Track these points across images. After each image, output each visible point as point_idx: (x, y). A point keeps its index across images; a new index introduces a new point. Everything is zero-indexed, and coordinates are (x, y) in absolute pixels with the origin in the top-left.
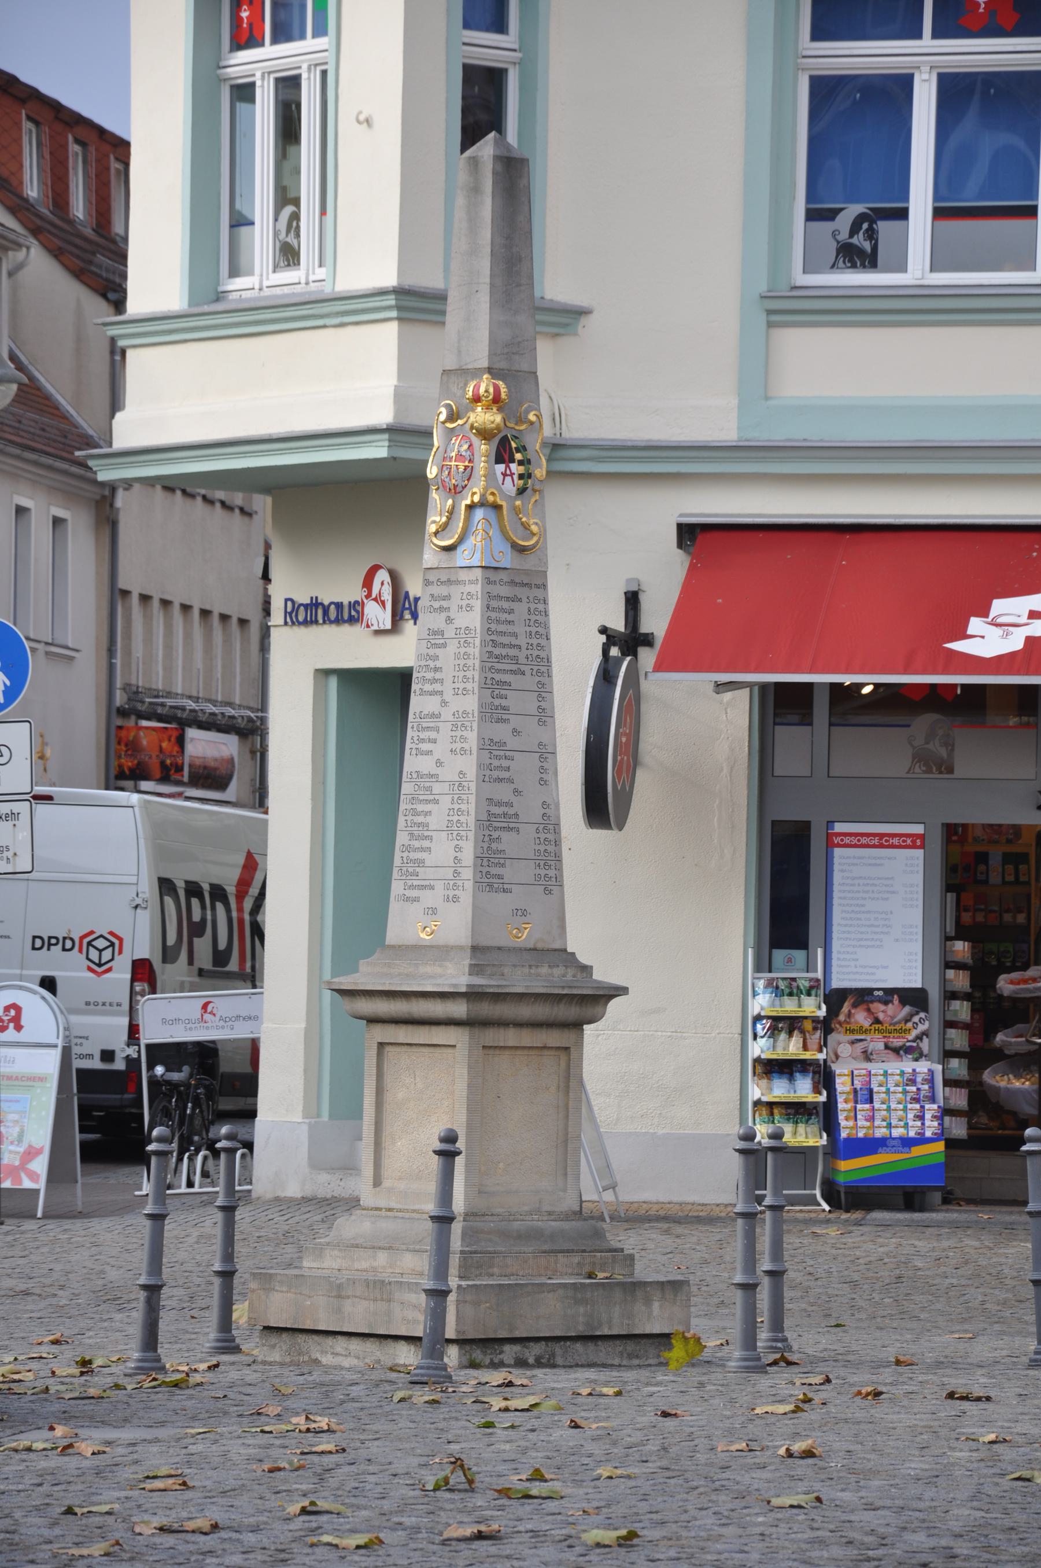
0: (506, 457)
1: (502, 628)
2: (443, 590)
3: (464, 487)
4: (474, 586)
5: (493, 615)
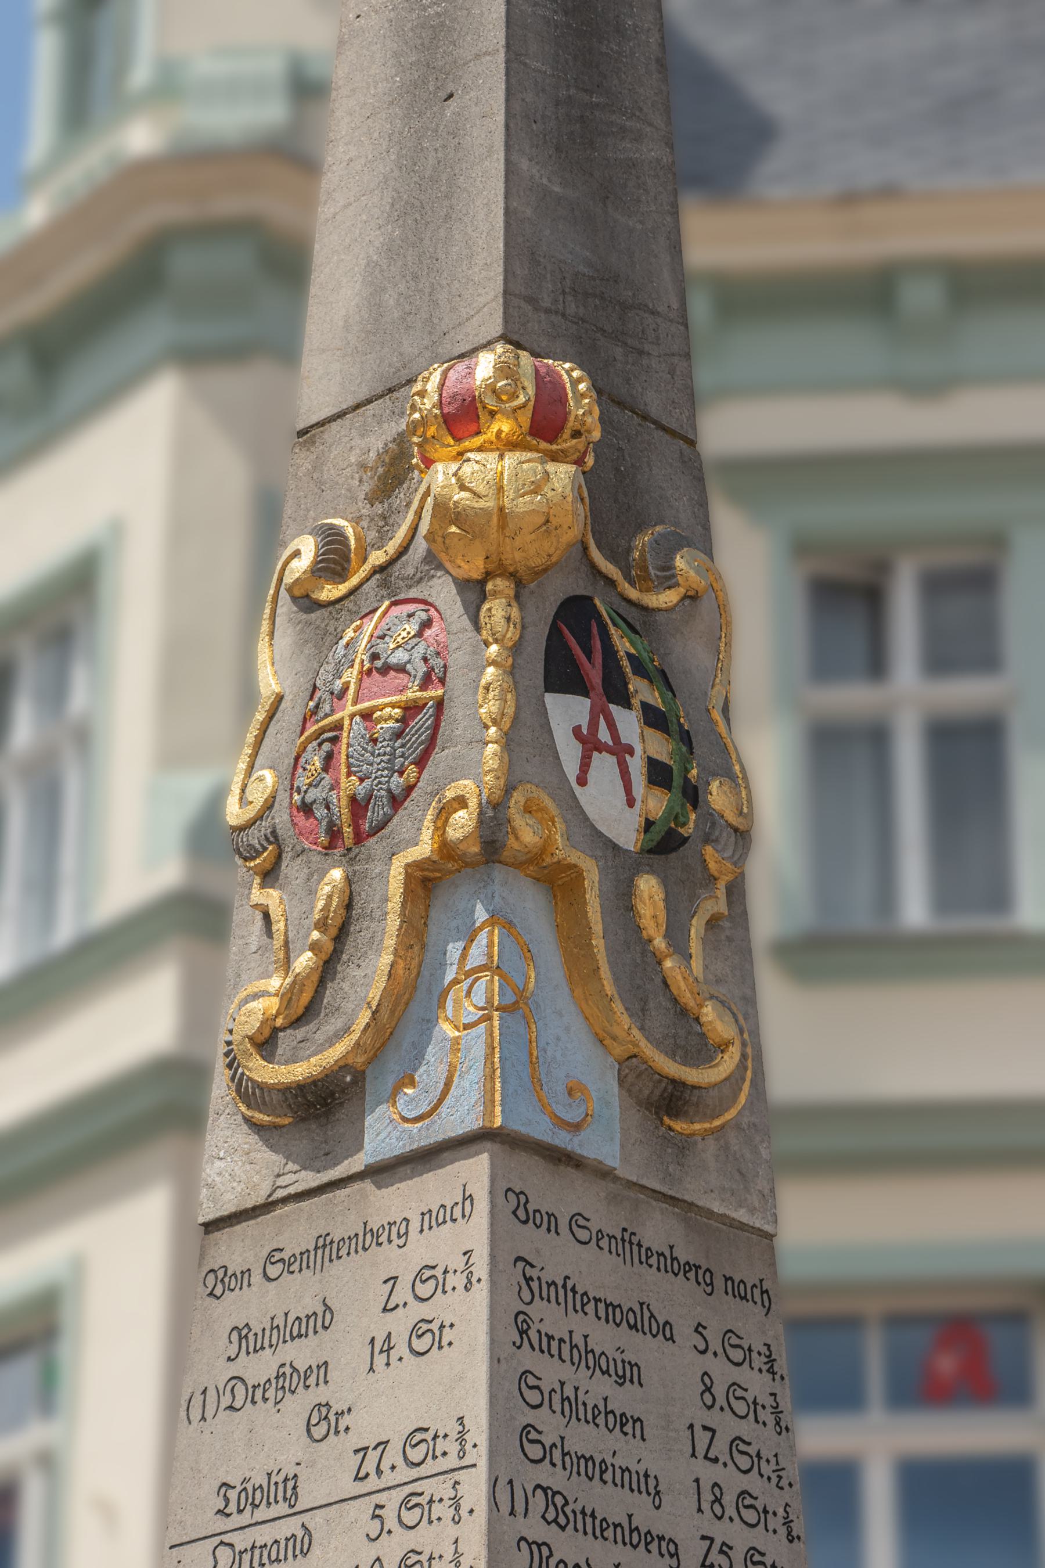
0: (594, 674)
1: (585, 1439)
2: (299, 1295)
3: (396, 802)
4: (448, 1232)
5: (551, 1372)
